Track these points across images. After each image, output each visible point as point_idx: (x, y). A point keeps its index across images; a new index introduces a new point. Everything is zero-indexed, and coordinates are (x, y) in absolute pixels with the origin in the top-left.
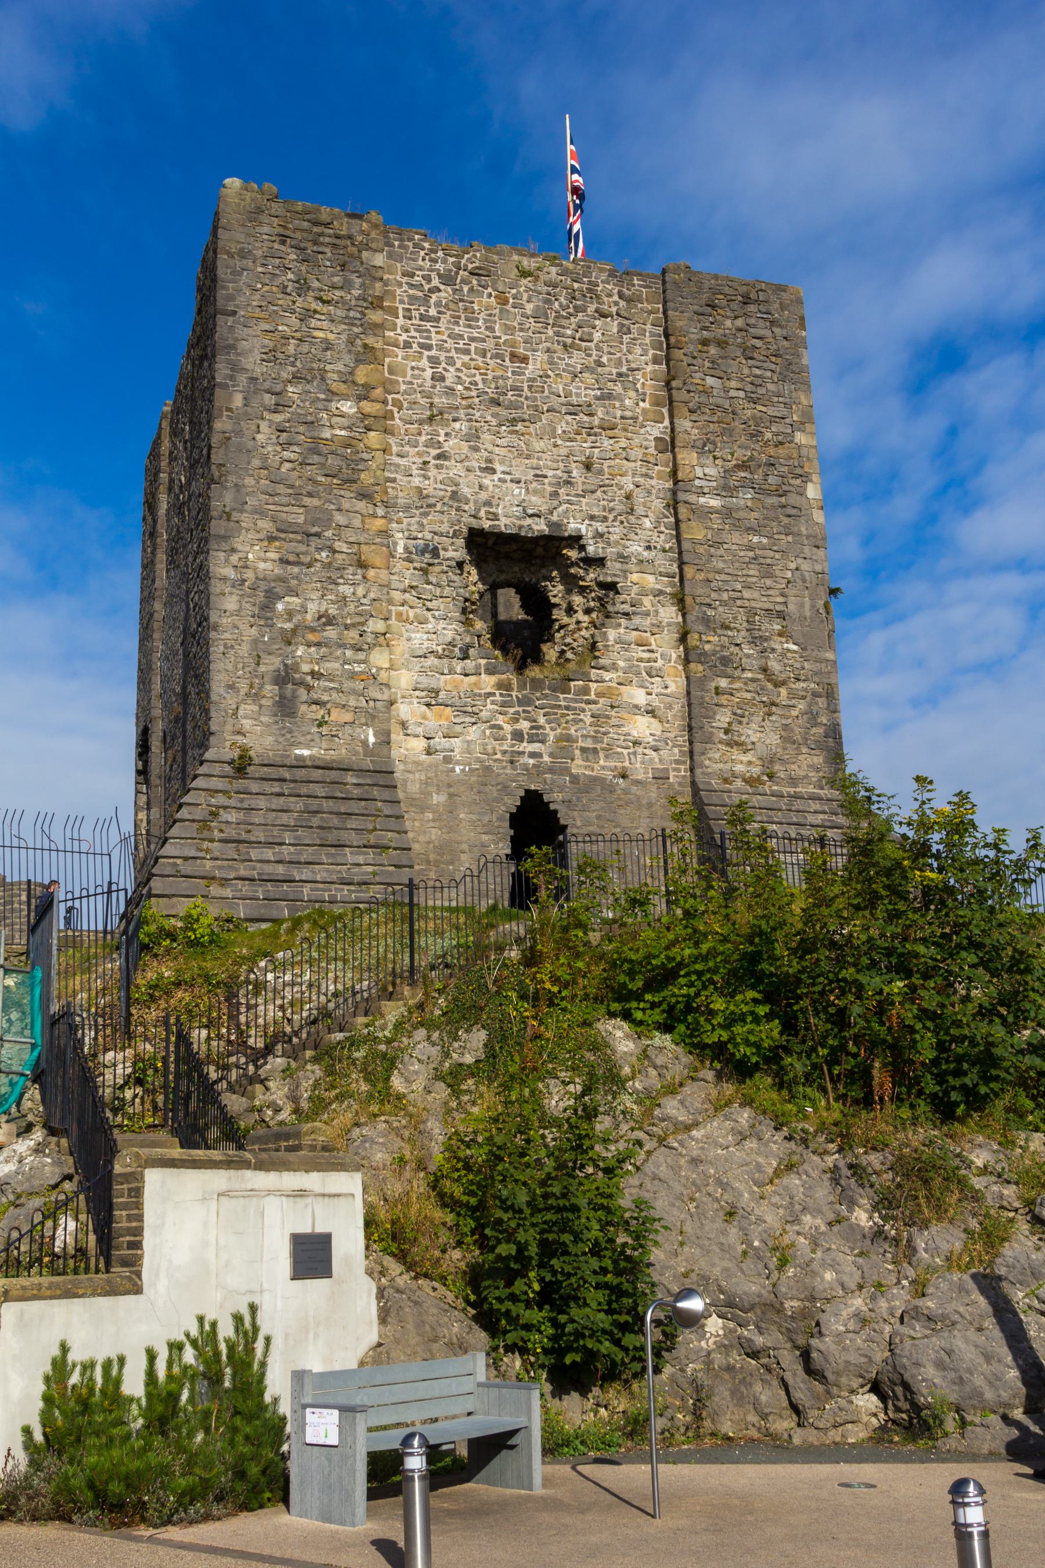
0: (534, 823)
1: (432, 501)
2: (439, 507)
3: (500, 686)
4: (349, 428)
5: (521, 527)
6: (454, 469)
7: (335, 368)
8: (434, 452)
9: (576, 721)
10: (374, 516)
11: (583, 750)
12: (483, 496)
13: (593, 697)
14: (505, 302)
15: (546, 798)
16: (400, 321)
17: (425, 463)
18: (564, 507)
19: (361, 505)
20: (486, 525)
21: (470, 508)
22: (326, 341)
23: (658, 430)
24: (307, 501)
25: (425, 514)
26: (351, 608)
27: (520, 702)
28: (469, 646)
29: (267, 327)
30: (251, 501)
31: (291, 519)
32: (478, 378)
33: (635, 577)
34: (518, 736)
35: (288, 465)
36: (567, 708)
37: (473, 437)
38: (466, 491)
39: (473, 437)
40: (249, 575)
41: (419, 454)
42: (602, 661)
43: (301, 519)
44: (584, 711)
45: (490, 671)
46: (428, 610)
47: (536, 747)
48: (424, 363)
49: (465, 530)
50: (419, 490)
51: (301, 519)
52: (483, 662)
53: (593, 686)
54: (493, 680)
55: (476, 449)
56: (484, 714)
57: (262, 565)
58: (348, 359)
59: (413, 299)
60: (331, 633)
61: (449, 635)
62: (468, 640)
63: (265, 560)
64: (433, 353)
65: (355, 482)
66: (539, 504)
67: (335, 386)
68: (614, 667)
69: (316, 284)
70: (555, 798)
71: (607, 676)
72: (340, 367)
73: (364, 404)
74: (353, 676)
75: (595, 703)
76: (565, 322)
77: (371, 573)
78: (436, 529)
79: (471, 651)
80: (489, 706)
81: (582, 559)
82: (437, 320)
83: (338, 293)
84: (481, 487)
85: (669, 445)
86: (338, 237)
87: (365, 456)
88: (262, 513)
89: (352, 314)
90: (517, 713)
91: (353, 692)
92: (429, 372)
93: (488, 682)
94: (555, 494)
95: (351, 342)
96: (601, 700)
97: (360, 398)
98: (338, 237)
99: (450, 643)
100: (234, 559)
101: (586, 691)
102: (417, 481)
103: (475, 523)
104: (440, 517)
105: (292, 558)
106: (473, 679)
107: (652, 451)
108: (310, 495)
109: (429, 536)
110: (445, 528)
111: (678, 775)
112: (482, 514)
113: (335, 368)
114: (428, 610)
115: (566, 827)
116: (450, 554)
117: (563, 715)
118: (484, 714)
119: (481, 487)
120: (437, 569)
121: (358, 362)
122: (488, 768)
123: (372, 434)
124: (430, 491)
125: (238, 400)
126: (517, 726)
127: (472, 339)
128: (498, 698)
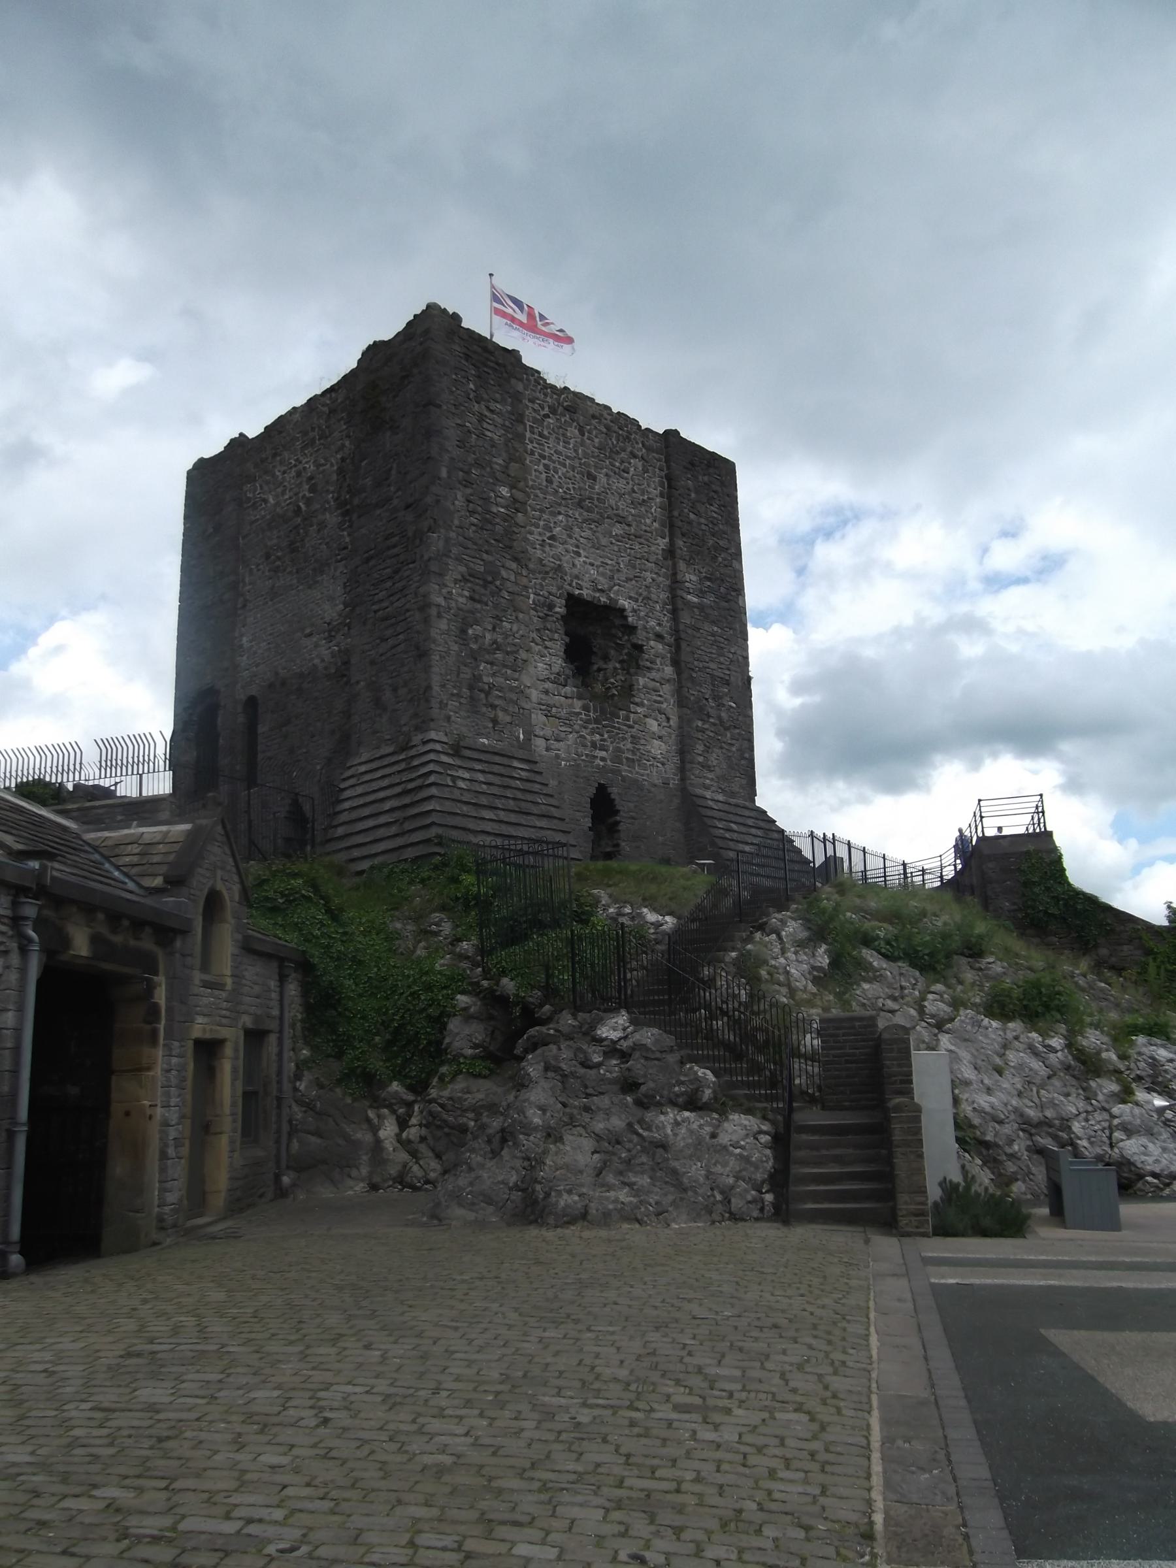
0: (603, 806)
1: (548, 569)
4: (506, 507)
8: (548, 534)
11: (627, 758)
14: (583, 435)
15: (609, 790)
16: (528, 434)
18: (616, 588)
19: (514, 565)
22: (492, 439)
23: (663, 543)
24: (485, 556)
25: (544, 579)
26: (510, 640)
29: (459, 422)
30: (455, 550)
31: (477, 567)
32: (571, 486)
33: (652, 643)
34: (594, 745)
35: (474, 528)
40: (453, 605)
42: (637, 700)
43: (482, 569)
45: (580, 698)
46: (546, 648)
47: (604, 754)
48: (541, 468)
51: (482, 569)
55: (571, 537)
57: (461, 600)
59: (535, 421)
60: (499, 655)
63: (462, 596)
64: (546, 462)
65: (511, 548)
66: (603, 583)
68: (641, 705)
70: (614, 791)
71: (639, 710)
73: (514, 491)
74: (511, 689)
76: (616, 457)
81: (622, 626)
82: (548, 438)
85: (670, 553)
88: (459, 559)
91: (511, 701)
92: (544, 476)
93: (578, 705)
94: (612, 578)
100: (444, 591)
105: (477, 597)
106: (570, 701)
107: (660, 557)
108: (487, 552)
111: (674, 782)
114: (546, 648)
115: (618, 811)
120: (550, 618)
122: (579, 765)
123: (520, 514)
125: (444, 473)
127: (568, 457)
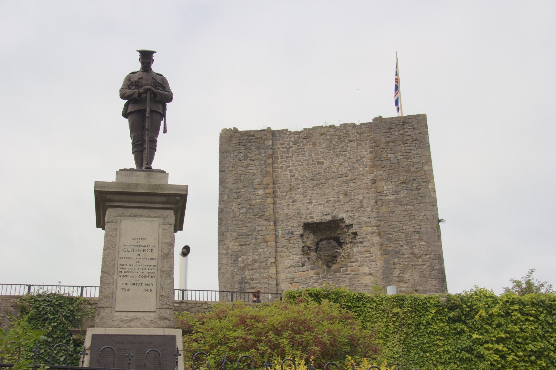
1: (291, 216)
2: (293, 218)
3: (315, 274)
5: (322, 219)
6: (298, 205)
7: (256, 181)
9: (343, 282)
10: (270, 225)
12: (309, 211)
13: (349, 272)
17: (288, 205)
19: (265, 223)
20: (310, 221)
21: (304, 216)
27: (323, 278)
28: (304, 262)
36: (339, 277)
37: (304, 194)
38: (302, 211)
39: (304, 194)
41: (286, 202)
42: (352, 260)
44: (345, 277)
45: (312, 269)
49: (302, 224)
50: (287, 214)
52: (310, 266)
53: (349, 269)
54: (313, 272)
56: (310, 284)
58: (261, 177)
61: (297, 260)
62: (304, 260)
67: (256, 187)
68: (357, 261)
69: (250, 155)
71: (353, 264)
72: (258, 180)
75: (350, 274)
77: (269, 244)
78: (292, 225)
79: (306, 264)
80: (312, 281)
83: (257, 156)
84: (307, 209)
86: (257, 139)
87: (267, 207)
89: (262, 162)
90: (322, 282)
93: (311, 273)
95: (261, 171)
96: (352, 273)
97: (265, 188)
98: (257, 139)
99: (298, 262)
101: (347, 271)
102: (286, 211)
103: (306, 221)
104: (294, 221)
106: (306, 273)
109: (290, 228)
110: (295, 225)
112: (308, 217)
113: (256, 181)
116: (297, 233)
117: (338, 280)
118: (310, 284)
119: (307, 209)
120: (293, 238)
121: (264, 177)
124: (290, 213)
126: (322, 286)
128: (315, 278)
